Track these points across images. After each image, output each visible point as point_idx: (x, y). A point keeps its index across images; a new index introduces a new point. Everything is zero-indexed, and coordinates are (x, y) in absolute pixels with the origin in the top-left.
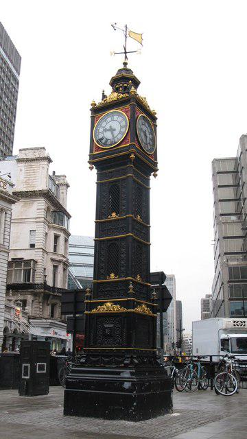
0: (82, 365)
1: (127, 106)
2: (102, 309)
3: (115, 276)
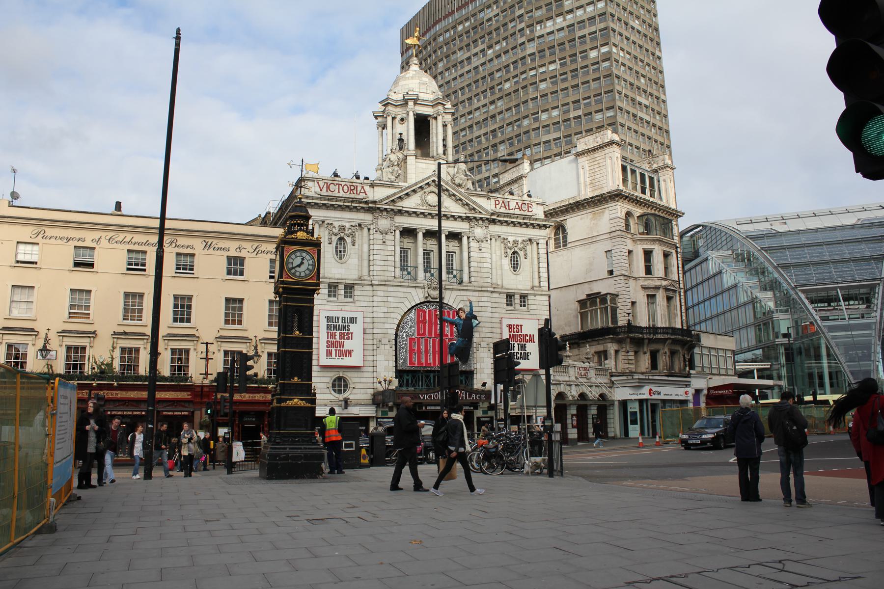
0: (278, 444)
1: (315, 249)
2: (289, 403)
3: (298, 379)
